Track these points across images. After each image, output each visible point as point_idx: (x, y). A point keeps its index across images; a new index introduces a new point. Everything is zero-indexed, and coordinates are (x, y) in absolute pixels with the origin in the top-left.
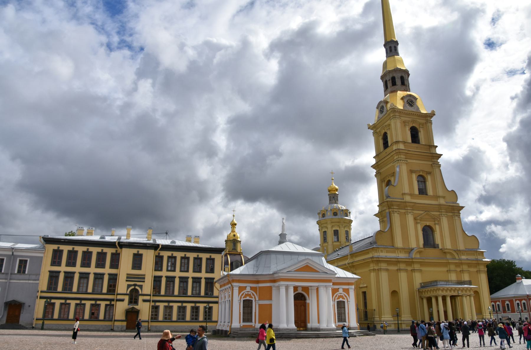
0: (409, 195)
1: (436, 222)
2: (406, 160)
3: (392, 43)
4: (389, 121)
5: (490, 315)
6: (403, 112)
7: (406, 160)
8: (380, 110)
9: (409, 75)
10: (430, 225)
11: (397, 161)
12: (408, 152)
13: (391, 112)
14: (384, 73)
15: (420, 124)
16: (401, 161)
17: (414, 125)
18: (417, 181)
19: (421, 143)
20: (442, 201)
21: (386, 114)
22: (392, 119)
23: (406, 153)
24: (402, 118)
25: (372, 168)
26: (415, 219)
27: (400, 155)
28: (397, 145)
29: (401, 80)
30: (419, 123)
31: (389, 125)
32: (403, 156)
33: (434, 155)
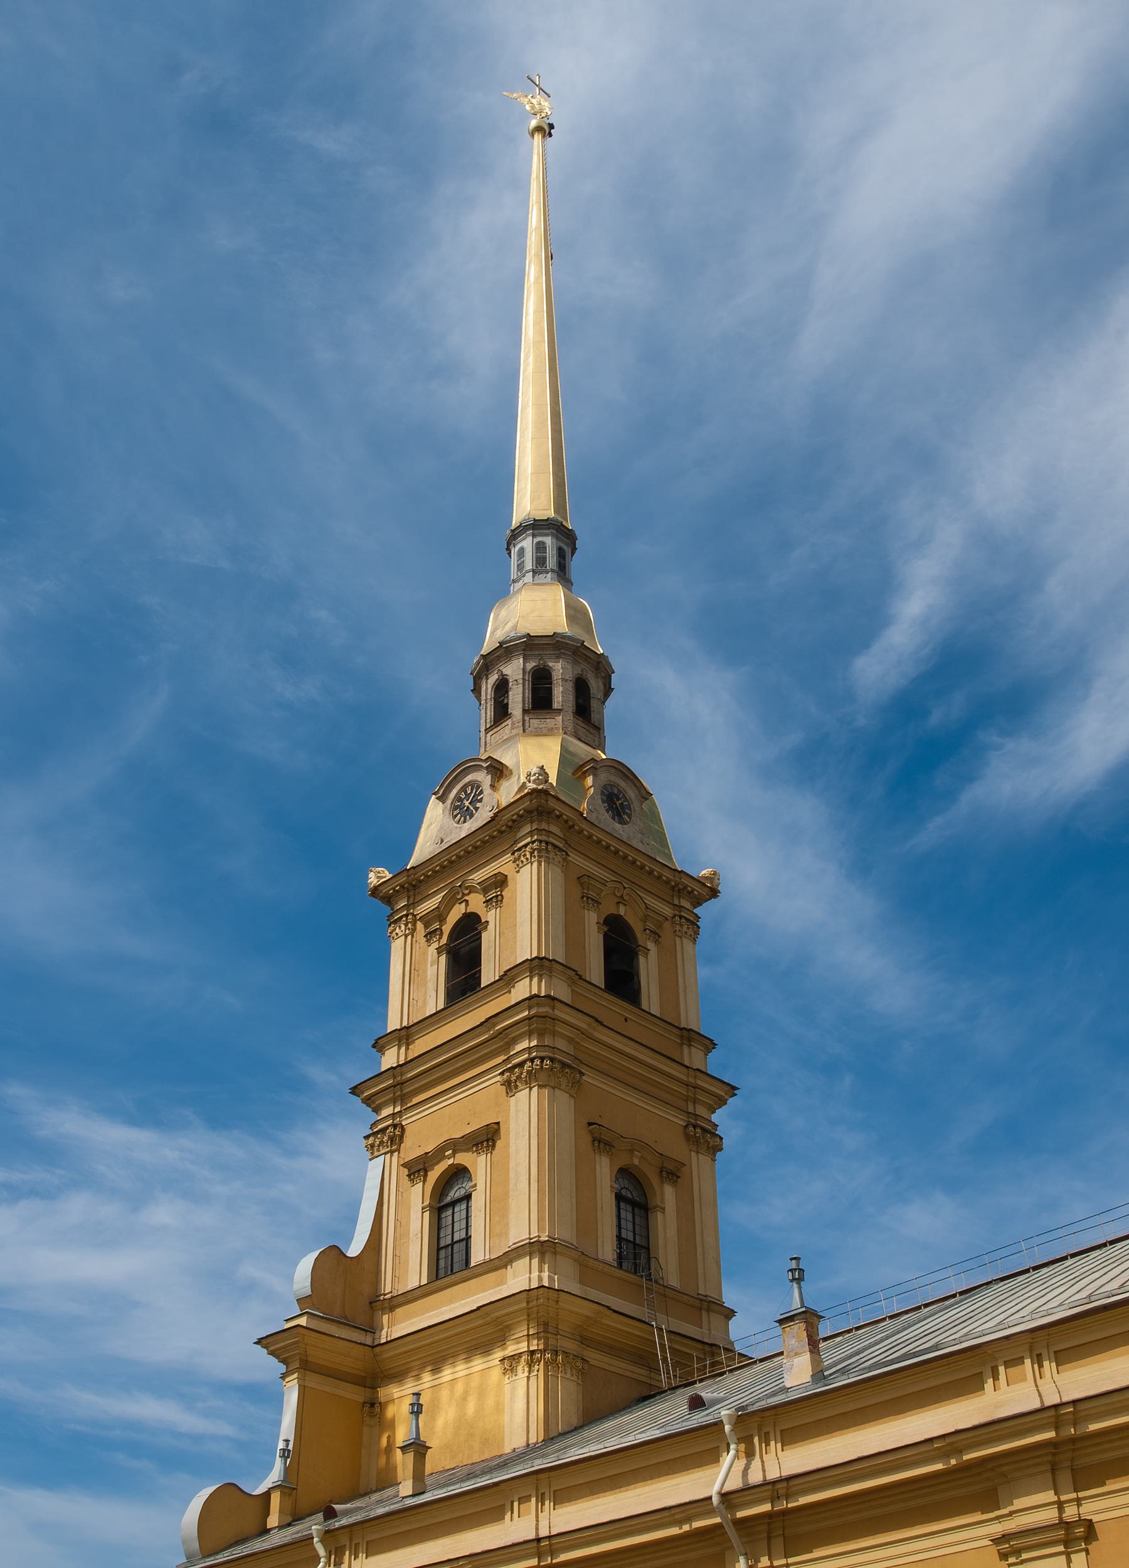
0: (575, 1260)
4: (508, 857)
8: (456, 808)
9: (608, 690)
11: (532, 1060)
13: (528, 812)
14: (501, 643)
17: (622, 911)
21: (493, 819)
22: (526, 846)
25: (357, 1101)
27: (554, 1034)
28: (535, 980)
30: (647, 908)
31: (501, 881)
33: (699, 1082)
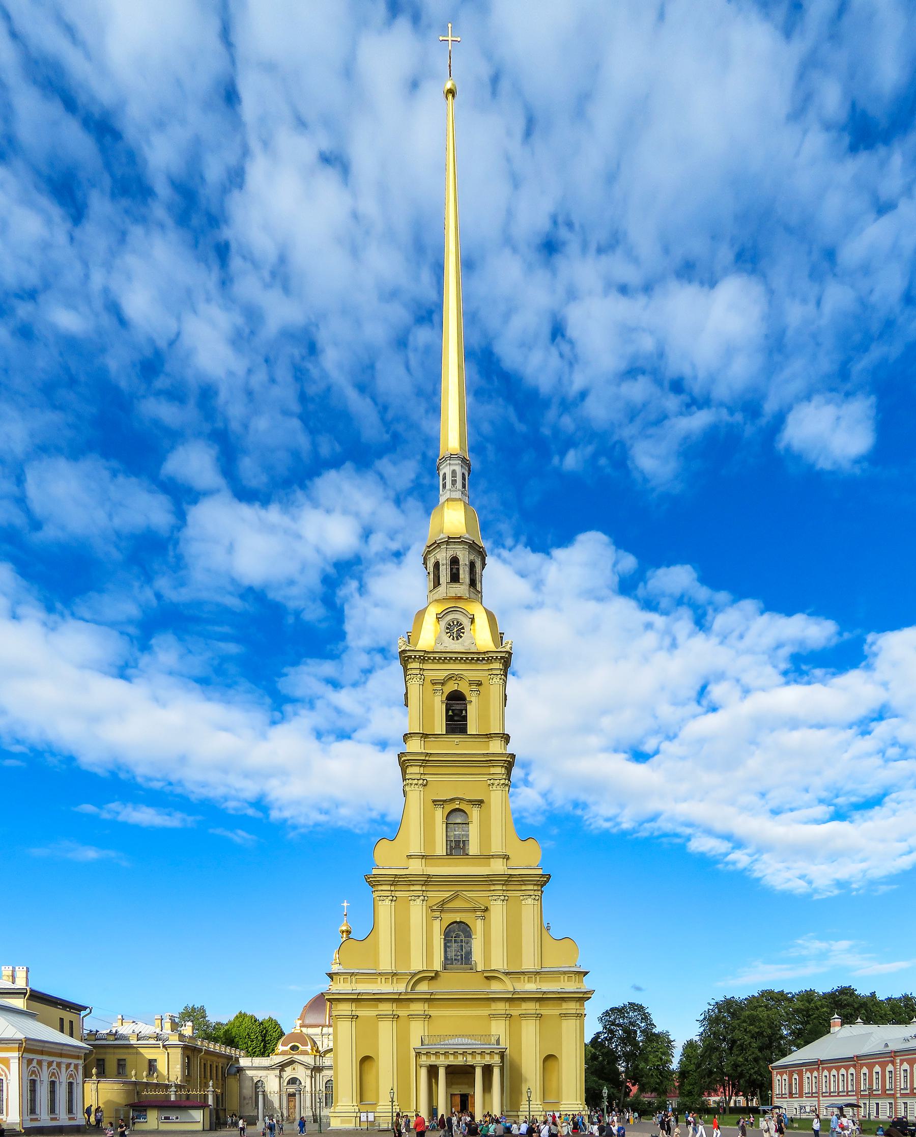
1: (479, 914)
2: (422, 777)
7: (422, 777)
20: (498, 867)
29: (451, 569)
32: (415, 770)
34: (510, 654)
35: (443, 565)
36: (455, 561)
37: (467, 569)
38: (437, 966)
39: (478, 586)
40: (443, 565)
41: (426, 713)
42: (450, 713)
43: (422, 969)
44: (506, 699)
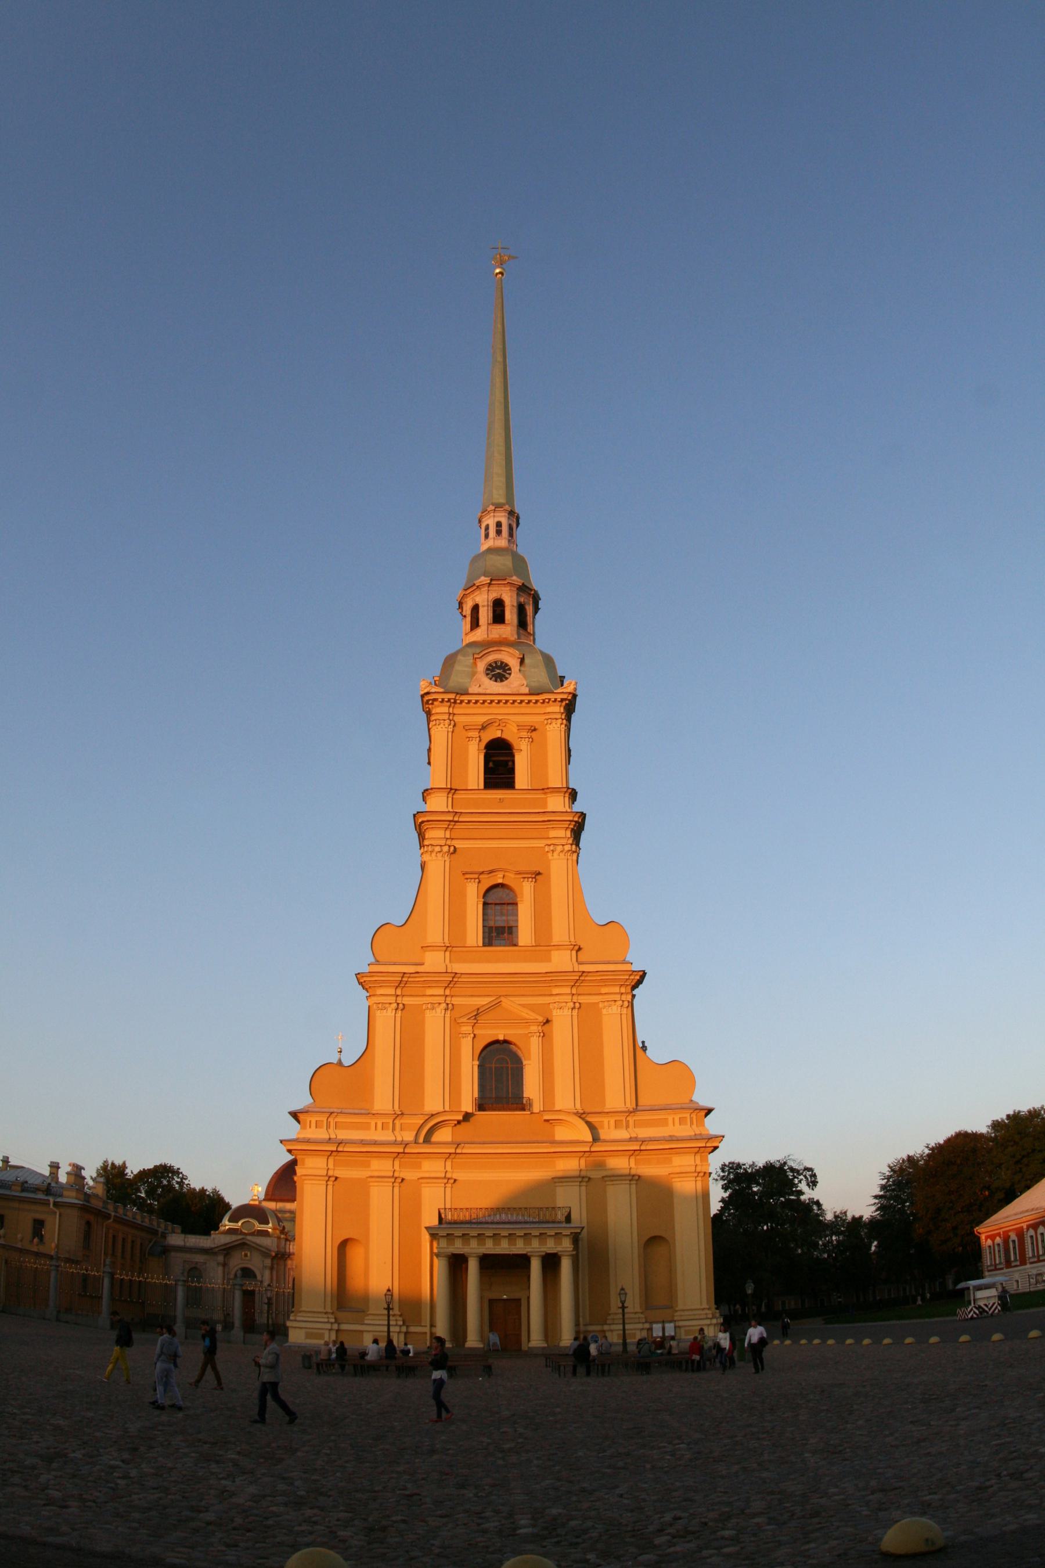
2: (449, 842)
3: (492, 514)
5: (623, 1311)
6: (462, 702)
7: (449, 842)
10: (506, 1038)
12: (456, 819)
15: (520, 727)
16: (430, 849)
17: (498, 734)
18: (485, 904)
19: (517, 786)
20: (562, 961)
23: (450, 821)
24: (456, 718)
26: (455, 1022)
29: (494, 611)
30: (518, 726)
32: (440, 833)
34: (575, 696)
35: (483, 606)
36: (498, 605)
37: (515, 610)
38: (468, 1106)
39: (530, 628)
40: (483, 606)
41: (455, 760)
42: (491, 765)
43: (442, 1109)
44: (570, 756)
